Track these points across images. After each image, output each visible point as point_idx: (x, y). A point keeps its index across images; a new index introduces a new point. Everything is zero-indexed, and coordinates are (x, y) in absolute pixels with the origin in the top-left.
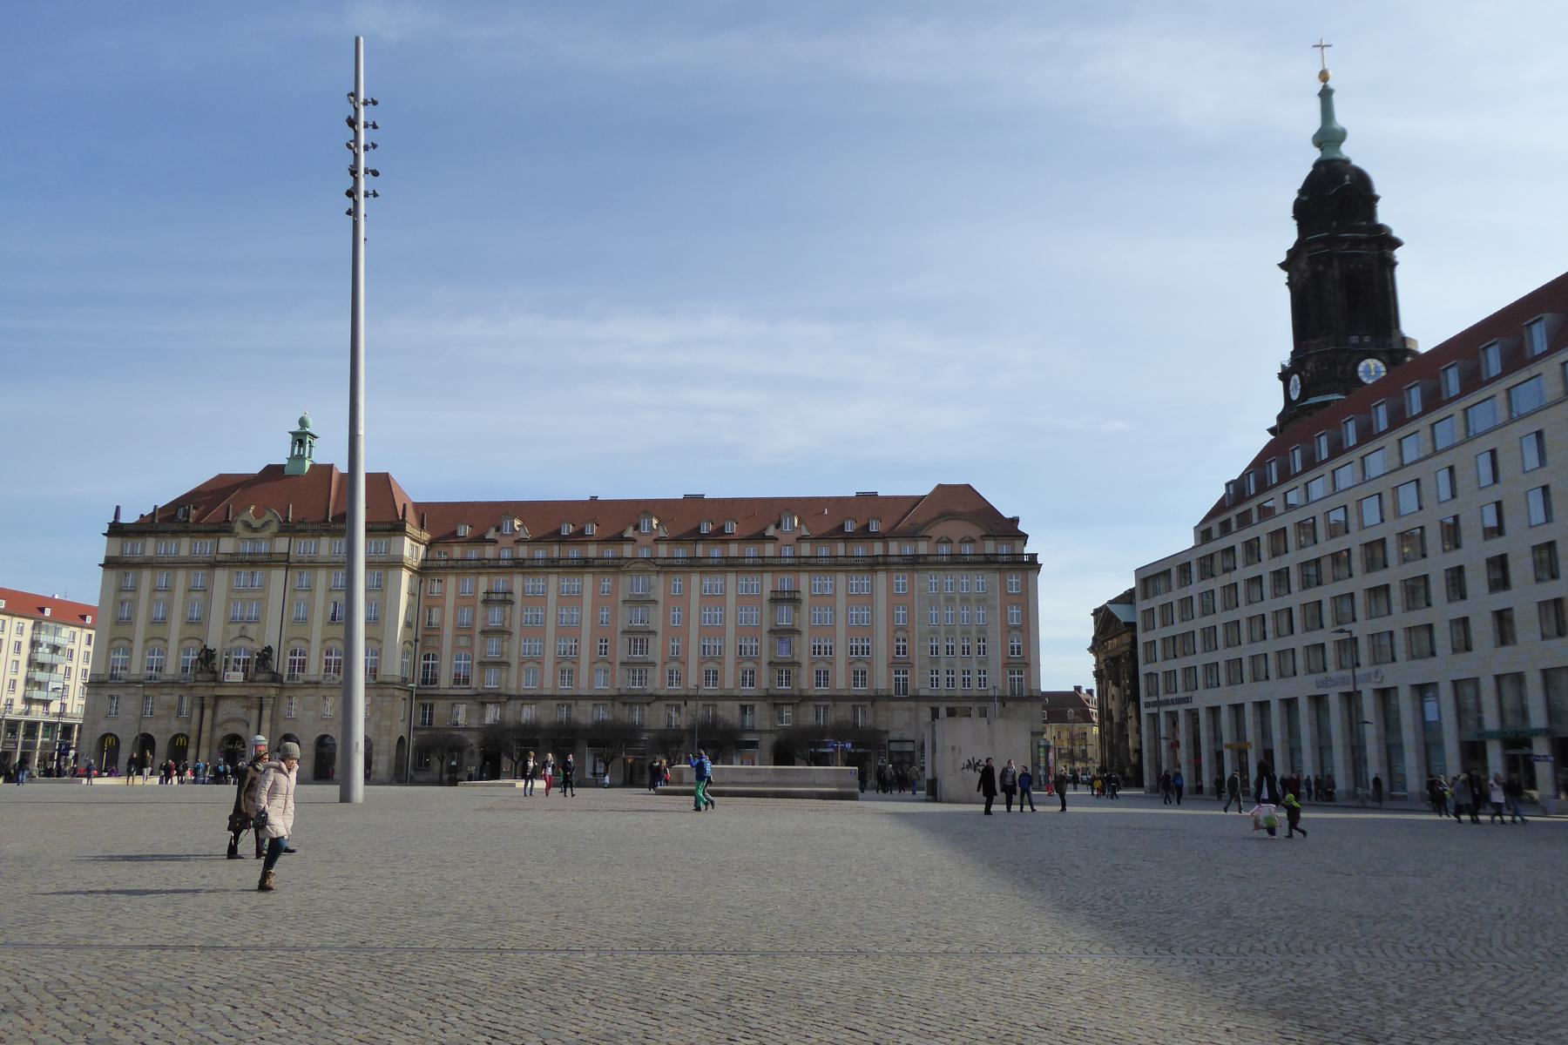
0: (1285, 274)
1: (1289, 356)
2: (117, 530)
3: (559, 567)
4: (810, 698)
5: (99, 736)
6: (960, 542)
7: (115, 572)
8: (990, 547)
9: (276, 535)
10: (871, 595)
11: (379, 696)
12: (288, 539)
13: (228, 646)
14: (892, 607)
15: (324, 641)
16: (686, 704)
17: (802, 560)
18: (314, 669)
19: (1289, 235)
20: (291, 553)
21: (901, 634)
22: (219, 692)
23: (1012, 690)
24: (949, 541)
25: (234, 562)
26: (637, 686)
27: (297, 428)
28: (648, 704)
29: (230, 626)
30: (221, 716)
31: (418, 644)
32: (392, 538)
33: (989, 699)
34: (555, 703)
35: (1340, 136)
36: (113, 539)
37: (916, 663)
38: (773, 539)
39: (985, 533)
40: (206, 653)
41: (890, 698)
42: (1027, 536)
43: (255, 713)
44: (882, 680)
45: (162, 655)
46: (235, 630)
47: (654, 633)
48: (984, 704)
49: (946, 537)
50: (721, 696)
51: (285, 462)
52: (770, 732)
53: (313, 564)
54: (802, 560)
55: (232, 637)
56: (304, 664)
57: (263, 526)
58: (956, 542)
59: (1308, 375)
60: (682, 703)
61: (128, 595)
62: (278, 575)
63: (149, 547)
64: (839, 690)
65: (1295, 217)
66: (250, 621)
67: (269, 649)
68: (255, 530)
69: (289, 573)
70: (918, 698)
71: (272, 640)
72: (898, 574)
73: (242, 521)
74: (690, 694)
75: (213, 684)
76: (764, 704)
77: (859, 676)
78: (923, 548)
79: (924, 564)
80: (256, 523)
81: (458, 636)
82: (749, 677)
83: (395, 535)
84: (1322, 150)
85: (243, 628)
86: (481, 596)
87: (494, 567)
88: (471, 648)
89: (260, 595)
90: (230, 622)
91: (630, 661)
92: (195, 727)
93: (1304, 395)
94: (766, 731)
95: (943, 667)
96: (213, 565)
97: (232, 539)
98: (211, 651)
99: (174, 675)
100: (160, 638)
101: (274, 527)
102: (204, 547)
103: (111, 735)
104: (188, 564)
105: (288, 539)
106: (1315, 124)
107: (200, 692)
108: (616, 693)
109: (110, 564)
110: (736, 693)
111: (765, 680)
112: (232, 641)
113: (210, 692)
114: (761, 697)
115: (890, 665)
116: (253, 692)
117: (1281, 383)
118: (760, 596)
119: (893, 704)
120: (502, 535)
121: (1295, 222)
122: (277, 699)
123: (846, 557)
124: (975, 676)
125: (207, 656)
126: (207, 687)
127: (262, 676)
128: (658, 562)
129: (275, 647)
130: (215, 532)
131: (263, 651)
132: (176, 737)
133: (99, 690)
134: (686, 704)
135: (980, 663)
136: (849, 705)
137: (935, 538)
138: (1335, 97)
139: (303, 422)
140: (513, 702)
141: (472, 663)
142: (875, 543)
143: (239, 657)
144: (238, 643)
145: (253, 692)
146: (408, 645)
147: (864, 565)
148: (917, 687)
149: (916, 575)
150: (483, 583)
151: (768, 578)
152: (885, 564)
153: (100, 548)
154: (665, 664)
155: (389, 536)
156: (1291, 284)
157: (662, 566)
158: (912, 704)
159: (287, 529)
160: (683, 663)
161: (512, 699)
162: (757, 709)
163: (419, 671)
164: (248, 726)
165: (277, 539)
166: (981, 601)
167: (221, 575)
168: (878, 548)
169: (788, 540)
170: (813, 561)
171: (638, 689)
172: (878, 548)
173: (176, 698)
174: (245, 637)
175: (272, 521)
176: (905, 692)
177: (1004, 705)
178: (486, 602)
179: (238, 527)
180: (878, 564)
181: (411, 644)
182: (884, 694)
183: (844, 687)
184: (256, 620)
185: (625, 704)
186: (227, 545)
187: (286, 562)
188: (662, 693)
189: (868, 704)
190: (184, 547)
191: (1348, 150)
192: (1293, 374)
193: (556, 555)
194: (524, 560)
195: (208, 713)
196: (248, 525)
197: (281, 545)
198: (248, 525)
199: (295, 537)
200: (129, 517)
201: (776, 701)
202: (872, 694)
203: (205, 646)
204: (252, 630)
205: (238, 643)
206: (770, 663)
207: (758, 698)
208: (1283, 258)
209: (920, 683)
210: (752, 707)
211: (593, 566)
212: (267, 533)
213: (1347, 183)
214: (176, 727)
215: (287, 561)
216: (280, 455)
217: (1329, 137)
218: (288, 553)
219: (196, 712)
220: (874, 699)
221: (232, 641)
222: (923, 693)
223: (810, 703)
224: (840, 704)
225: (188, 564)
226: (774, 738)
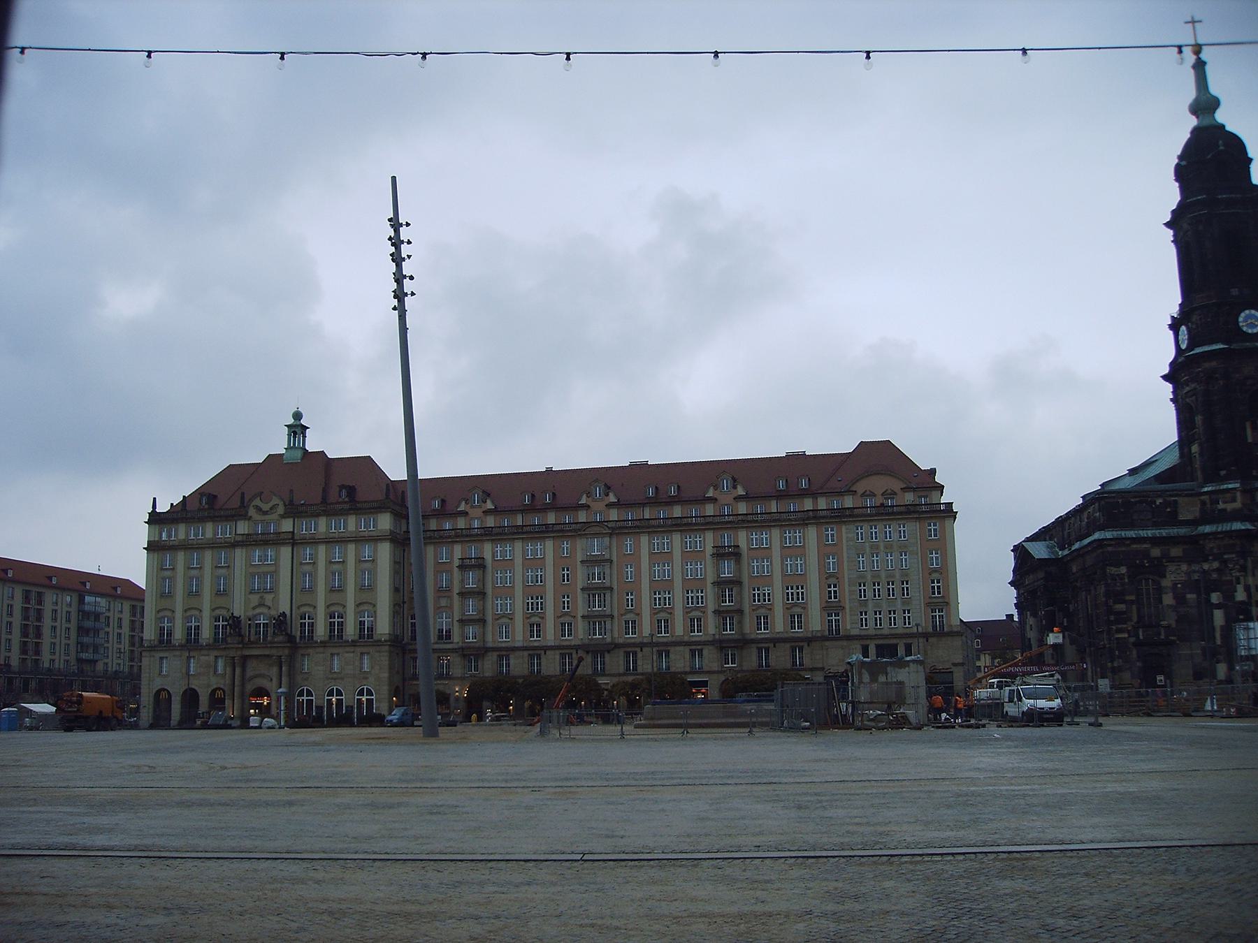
0: (1171, 232)
1: (1178, 308)
2: (155, 519)
3: (523, 533)
4: (753, 641)
5: (154, 691)
6: (882, 495)
8: (909, 498)
9: (283, 517)
10: (804, 546)
11: (377, 652)
12: (291, 520)
13: (250, 613)
14: (823, 557)
15: (328, 607)
16: (641, 651)
17: (740, 518)
18: (321, 631)
19: (1171, 196)
20: (295, 532)
21: (832, 581)
22: (247, 653)
23: (934, 627)
24: (873, 495)
25: (249, 542)
26: (597, 636)
27: (291, 421)
28: (609, 652)
29: (251, 596)
30: (249, 673)
31: (405, 605)
32: (379, 515)
33: (912, 636)
34: (526, 653)
35: (1214, 104)
36: (153, 526)
37: (847, 607)
38: (713, 500)
39: (905, 486)
40: (234, 621)
41: (824, 639)
42: (943, 486)
43: (275, 670)
44: (815, 622)
46: (255, 599)
49: (870, 491)
50: (673, 642)
51: (284, 452)
52: (718, 672)
53: (314, 542)
54: (740, 518)
55: (252, 605)
56: (312, 626)
57: (271, 509)
58: (879, 492)
59: (1194, 326)
60: (638, 650)
61: (168, 573)
62: (286, 551)
63: (181, 532)
64: (778, 633)
65: (1177, 180)
66: (266, 591)
67: (284, 614)
68: (265, 513)
69: (295, 549)
70: (849, 638)
71: (284, 607)
72: (827, 526)
73: (253, 506)
75: (240, 646)
76: (711, 648)
77: (795, 618)
78: (848, 502)
79: (850, 516)
80: (266, 507)
81: (439, 597)
82: (694, 623)
83: (381, 512)
84: (1197, 117)
85: (261, 597)
86: (457, 563)
87: (467, 536)
88: (451, 607)
89: (272, 569)
90: (251, 593)
91: (591, 614)
92: (228, 681)
93: (1191, 346)
94: (714, 672)
95: (870, 608)
97: (247, 522)
98: (237, 618)
99: (209, 639)
100: (196, 609)
101: (281, 510)
102: (224, 531)
103: (164, 690)
104: (214, 545)
105: (292, 519)
106: (1191, 94)
107: (232, 653)
108: (579, 643)
109: (152, 547)
110: (686, 638)
111: (711, 626)
112: (254, 608)
113: (239, 653)
114: (708, 641)
115: (824, 609)
116: (274, 652)
117: (1171, 332)
119: (827, 643)
120: (472, 507)
121: (1177, 184)
122: (292, 657)
123: (777, 513)
124: (899, 616)
125: (235, 622)
126: (237, 648)
127: (281, 638)
128: (613, 525)
129: (288, 613)
130: (233, 516)
131: (279, 616)
132: (214, 691)
133: (153, 653)
134: (641, 651)
135: (903, 603)
136: (788, 645)
137: (860, 492)
138: (1208, 68)
139: (297, 416)
140: (490, 654)
141: (453, 620)
142: (805, 500)
143: (304, 621)
144: (258, 611)
145: (274, 652)
146: (397, 607)
147: (796, 520)
148: (848, 628)
149: (844, 528)
150: (458, 551)
151: (709, 536)
152: (815, 518)
153: (142, 534)
154: (622, 615)
155: (377, 513)
156: (1176, 241)
157: (612, 528)
158: (845, 643)
159: (293, 510)
160: (638, 614)
161: (489, 651)
162: (705, 652)
163: (408, 628)
164: (271, 680)
165: (283, 520)
166: (903, 550)
167: (239, 554)
168: (808, 504)
169: (728, 501)
170: (750, 518)
171: (598, 638)
172: (808, 504)
173: (212, 658)
174: (264, 605)
176: (838, 631)
177: (927, 641)
178: (462, 567)
179: (252, 512)
180: (808, 519)
181: (399, 605)
182: (819, 635)
183: (782, 631)
184: (272, 591)
185: (588, 652)
186: (243, 528)
187: (293, 541)
188: (621, 641)
190: (209, 531)
191: (1221, 116)
192: (1181, 325)
193: (520, 523)
194: (492, 528)
195: (238, 671)
196: (259, 509)
197: (287, 525)
198: (259, 509)
199: (298, 517)
200: (163, 507)
201: (722, 645)
203: (232, 614)
204: (269, 598)
205: (258, 611)
206: (715, 612)
207: (705, 643)
208: (1168, 218)
209: (849, 624)
210: (701, 651)
211: (553, 532)
212: (274, 516)
213: (1222, 148)
214: (215, 682)
215: (293, 538)
216: (279, 445)
217: (1205, 105)
218: (293, 532)
219: (229, 670)
220: (810, 640)
221: (254, 608)
222: (855, 632)
223: (753, 645)
225: (214, 545)
226: (722, 678)
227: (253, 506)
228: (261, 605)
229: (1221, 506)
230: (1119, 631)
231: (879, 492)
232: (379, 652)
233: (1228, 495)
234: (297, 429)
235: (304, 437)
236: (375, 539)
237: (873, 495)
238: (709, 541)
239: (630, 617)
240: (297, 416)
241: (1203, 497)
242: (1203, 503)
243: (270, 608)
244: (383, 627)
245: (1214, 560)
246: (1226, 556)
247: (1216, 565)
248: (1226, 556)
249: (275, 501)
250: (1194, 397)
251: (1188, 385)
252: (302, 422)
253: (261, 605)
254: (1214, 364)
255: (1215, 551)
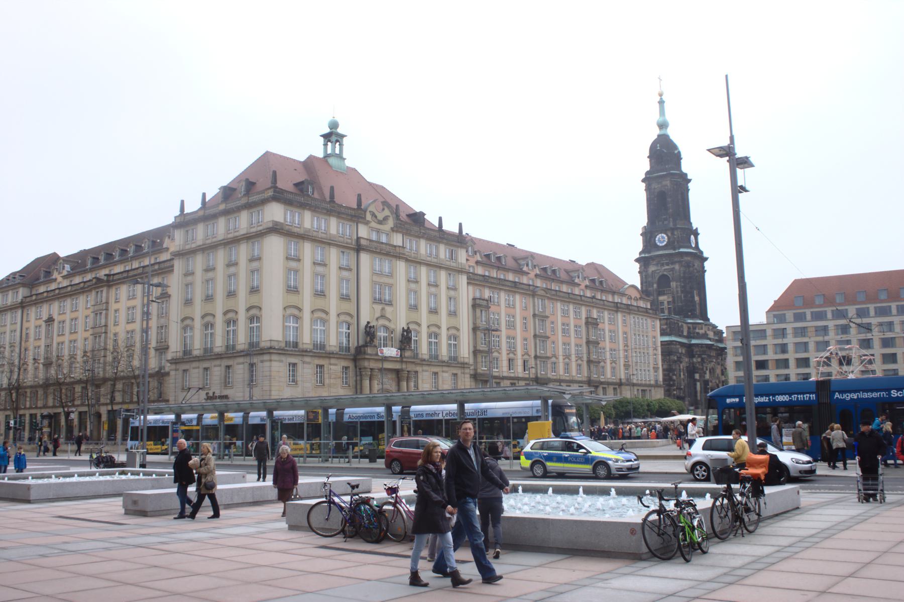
7: (182, 230)
29: (374, 306)
32: (459, 249)
44: (622, 375)
45: (314, 329)
47: (548, 338)
48: (650, 388)
73: (370, 212)
74: (561, 378)
85: (383, 309)
96: (358, 248)
108: (534, 377)
118: (581, 319)
139: (334, 125)
155: (458, 247)
175: (389, 216)
179: (369, 217)
184: (390, 303)
189: (617, 387)
202: (618, 381)
204: (389, 309)
224: (610, 386)
227: (370, 212)
228: (383, 316)
229: (697, 331)
230: (674, 390)
231: (633, 297)
232: (464, 373)
233: (700, 326)
234: (332, 136)
235: (341, 145)
236: (460, 271)
237: (631, 298)
238: (584, 311)
239: (554, 359)
240: (334, 125)
241: (690, 325)
242: (689, 328)
243: (389, 320)
244: (465, 352)
245: (698, 357)
246: (703, 356)
247: (699, 360)
248: (703, 356)
249: (387, 212)
250: (671, 272)
251: (668, 265)
252: (340, 130)
253: (383, 316)
254: (689, 259)
255: (698, 353)
